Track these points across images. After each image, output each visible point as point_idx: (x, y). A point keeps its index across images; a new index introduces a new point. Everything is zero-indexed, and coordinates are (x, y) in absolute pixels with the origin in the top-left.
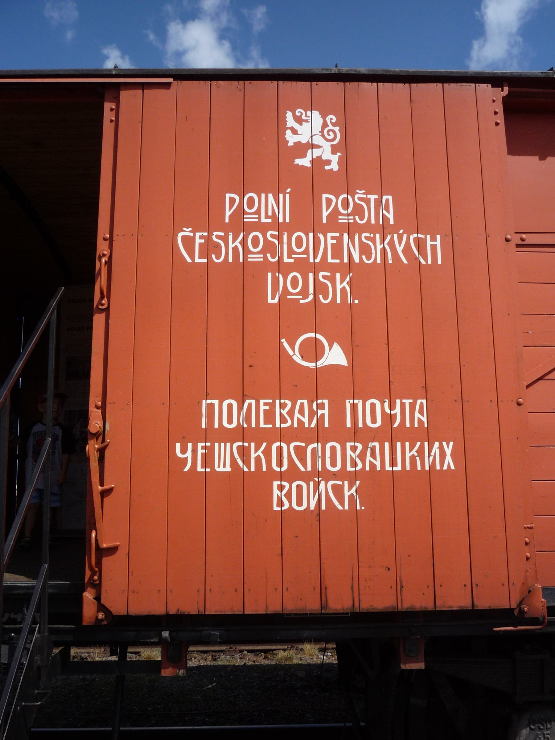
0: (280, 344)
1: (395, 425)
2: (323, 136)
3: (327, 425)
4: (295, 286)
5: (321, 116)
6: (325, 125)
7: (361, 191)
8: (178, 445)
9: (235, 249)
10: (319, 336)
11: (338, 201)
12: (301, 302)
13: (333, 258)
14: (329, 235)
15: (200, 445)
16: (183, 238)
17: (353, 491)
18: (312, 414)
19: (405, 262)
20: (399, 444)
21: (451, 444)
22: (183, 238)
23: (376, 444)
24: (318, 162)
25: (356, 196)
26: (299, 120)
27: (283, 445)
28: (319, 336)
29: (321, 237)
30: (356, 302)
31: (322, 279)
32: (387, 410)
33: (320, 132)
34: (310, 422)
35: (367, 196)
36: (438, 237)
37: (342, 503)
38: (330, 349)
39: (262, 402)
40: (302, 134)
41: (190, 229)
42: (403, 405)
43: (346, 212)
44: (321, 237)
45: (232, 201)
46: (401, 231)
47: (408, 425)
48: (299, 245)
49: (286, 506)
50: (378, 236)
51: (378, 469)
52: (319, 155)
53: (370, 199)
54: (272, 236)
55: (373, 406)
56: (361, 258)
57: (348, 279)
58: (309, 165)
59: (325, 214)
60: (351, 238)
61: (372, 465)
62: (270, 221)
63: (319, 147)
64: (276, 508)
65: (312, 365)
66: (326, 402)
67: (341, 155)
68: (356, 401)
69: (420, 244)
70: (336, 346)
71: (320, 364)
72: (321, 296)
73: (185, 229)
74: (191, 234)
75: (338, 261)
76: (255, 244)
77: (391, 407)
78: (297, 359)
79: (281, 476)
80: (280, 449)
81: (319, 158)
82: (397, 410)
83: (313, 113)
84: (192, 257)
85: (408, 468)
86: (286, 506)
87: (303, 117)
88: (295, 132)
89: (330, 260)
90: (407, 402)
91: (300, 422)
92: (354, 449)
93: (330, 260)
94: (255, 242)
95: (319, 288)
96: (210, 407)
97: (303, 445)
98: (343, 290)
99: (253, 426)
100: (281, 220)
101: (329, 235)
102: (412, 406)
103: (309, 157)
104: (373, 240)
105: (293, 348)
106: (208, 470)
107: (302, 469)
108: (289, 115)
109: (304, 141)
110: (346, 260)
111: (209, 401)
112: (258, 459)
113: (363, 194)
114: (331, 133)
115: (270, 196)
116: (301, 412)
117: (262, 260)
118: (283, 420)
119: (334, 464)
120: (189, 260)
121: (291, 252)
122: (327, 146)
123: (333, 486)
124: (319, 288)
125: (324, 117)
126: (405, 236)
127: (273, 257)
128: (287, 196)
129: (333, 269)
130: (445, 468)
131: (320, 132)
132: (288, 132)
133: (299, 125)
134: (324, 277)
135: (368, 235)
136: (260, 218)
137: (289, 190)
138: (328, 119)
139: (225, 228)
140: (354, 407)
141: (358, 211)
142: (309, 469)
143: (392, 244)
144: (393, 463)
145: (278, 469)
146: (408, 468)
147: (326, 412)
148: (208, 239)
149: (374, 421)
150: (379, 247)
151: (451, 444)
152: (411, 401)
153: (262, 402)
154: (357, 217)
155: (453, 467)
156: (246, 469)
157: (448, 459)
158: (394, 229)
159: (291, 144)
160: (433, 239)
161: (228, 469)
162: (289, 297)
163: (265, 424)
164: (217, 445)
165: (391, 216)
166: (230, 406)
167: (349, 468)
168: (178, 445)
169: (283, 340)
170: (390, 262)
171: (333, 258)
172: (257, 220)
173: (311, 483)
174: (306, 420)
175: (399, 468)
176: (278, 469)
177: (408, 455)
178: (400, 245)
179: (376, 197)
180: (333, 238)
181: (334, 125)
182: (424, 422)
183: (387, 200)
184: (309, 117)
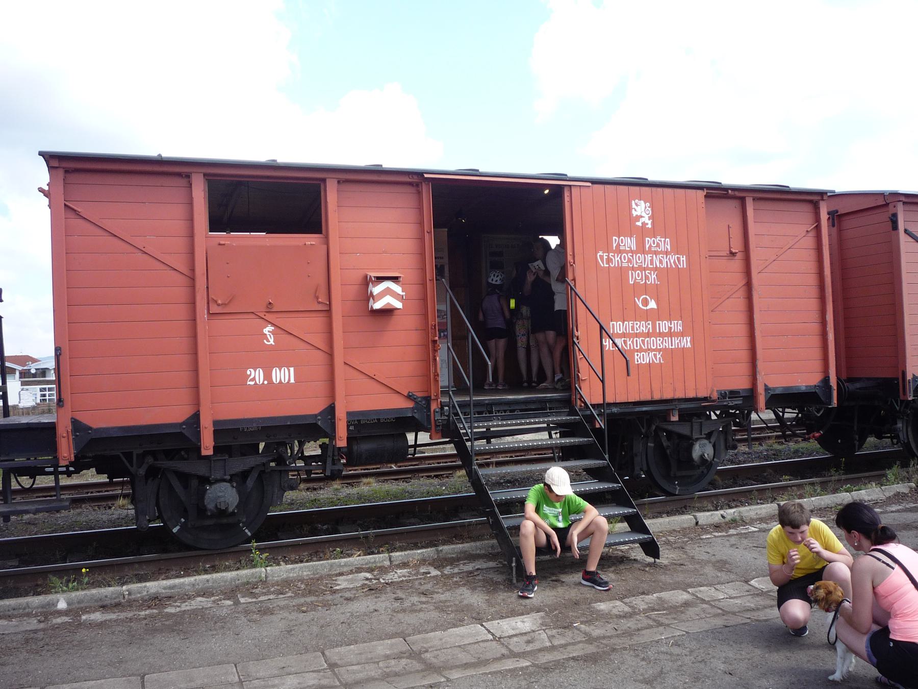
0: (635, 300)
4: (638, 276)
12: (641, 283)
18: (646, 327)
65: (645, 308)
78: (641, 305)
169: (636, 298)
174: (644, 329)
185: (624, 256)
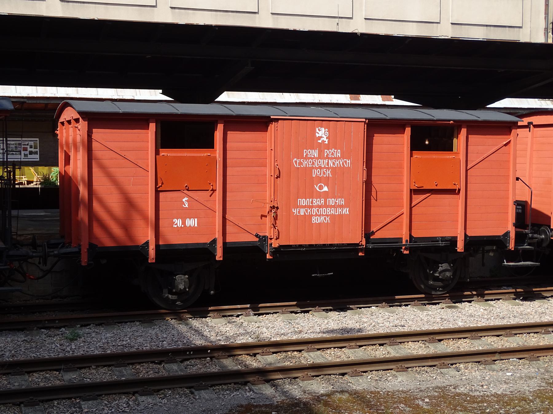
4: (318, 173)
6: (325, 132)
8: (293, 209)
10: (322, 184)
13: (327, 166)
14: (326, 160)
16: (295, 161)
18: (320, 202)
22: (295, 161)
23: (333, 209)
24: (323, 141)
26: (319, 130)
28: (322, 184)
29: (324, 160)
31: (324, 171)
36: (349, 160)
37: (326, 221)
39: (310, 199)
42: (339, 200)
43: (330, 154)
44: (324, 160)
49: (315, 222)
51: (333, 214)
55: (333, 200)
58: (321, 142)
61: (332, 213)
62: (313, 157)
63: (323, 137)
66: (323, 199)
69: (346, 162)
70: (326, 186)
71: (322, 191)
75: (328, 166)
76: (310, 163)
77: (337, 200)
78: (318, 189)
81: (323, 140)
82: (338, 201)
84: (297, 165)
88: (318, 133)
89: (326, 166)
90: (340, 199)
91: (318, 204)
93: (326, 166)
95: (324, 173)
98: (329, 173)
99: (308, 205)
101: (326, 160)
102: (341, 200)
103: (321, 140)
105: (317, 187)
108: (317, 129)
109: (320, 136)
110: (330, 166)
112: (309, 212)
119: (324, 213)
120: (296, 166)
122: (325, 137)
124: (324, 173)
125: (325, 129)
129: (327, 168)
130: (347, 214)
132: (317, 133)
134: (325, 170)
137: (318, 149)
139: (304, 158)
140: (329, 200)
141: (333, 154)
142: (320, 214)
143: (339, 162)
147: (323, 201)
149: (333, 203)
153: (310, 199)
155: (348, 214)
157: (348, 212)
158: (340, 158)
159: (317, 136)
160: (348, 161)
161: (303, 214)
166: (304, 200)
168: (293, 209)
171: (327, 166)
174: (319, 203)
175: (337, 214)
177: (339, 211)
180: (327, 161)
181: (327, 131)
185: (310, 161)
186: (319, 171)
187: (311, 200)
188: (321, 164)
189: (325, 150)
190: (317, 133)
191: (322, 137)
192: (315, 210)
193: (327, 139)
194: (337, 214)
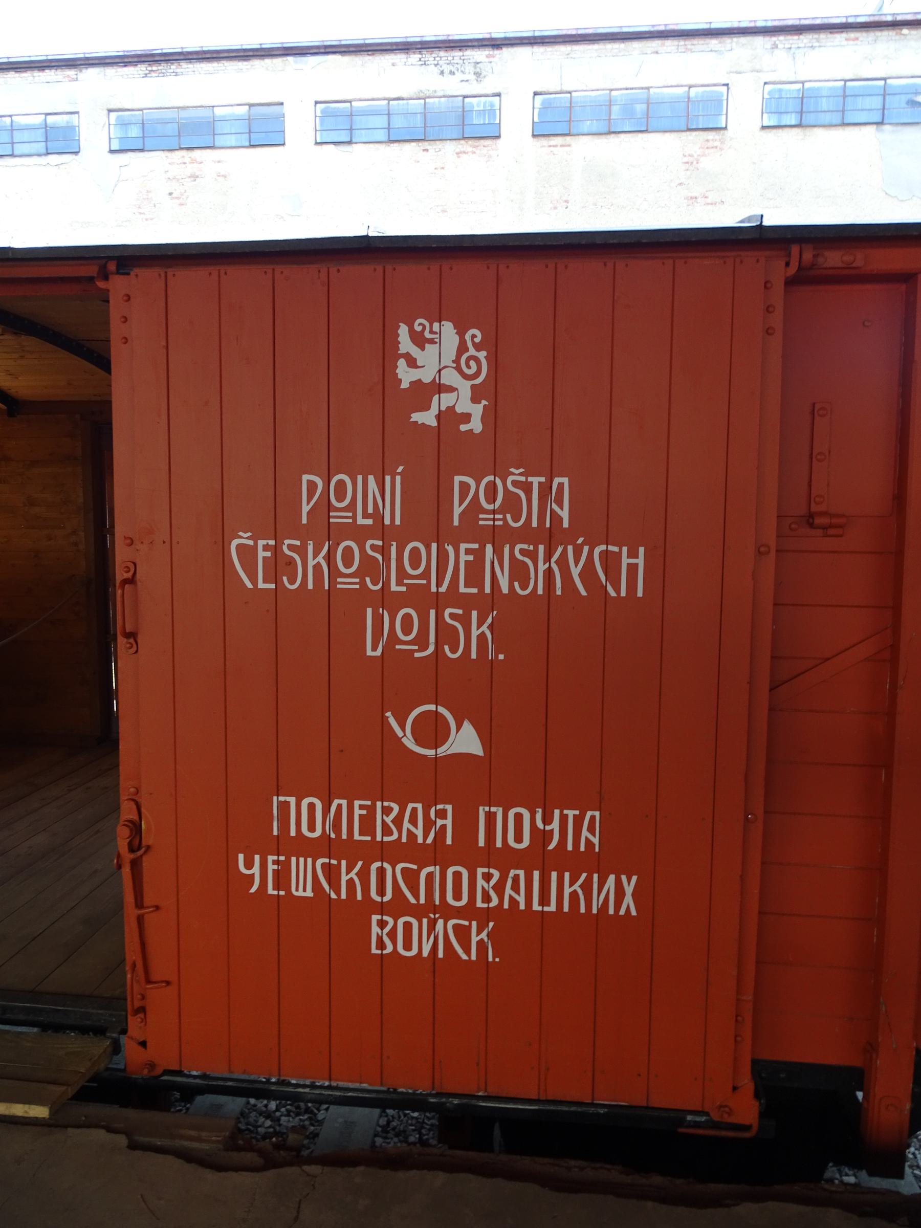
0: (384, 720)
1: (551, 847)
2: (458, 369)
3: (449, 841)
4: (407, 630)
5: (456, 331)
7: (517, 469)
8: (241, 857)
9: (317, 567)
10: (441, 710)
11: (478, 488)
12: (417, 655)
14: (463, 547)
15: (271, 858)
17: (484, 935)
18: (428, 824)
19: (584, 593)
20: (554, 875)
21: (634, 878)
22: (239, 547)
23: (521, 873)
24: (449, 417)
25: (510, 479)
26: (419, 340)
27: (386, 865)
28: (441, 710)
29: (450, 549)
30: (501, 657)
32: (540, 825)
33: (453, 362)
34: (425, 837)
35: (527, 479)
36: (642, 550)
37: (468, 951)
38: (458, 729)
39: (357, 803)
40: (424, 366)
41: (249, 534)
42: (564, 819)
43: (490, 507)
44: (450, 549)
45: (312, 486)
46: (580, 541)
47: (570, 847)
48: (415, 564)
49: (389, 949)
50: (541, 548)
51: (522, 907)
52: (451, 404)
53: (532, 483)
54: (373, 547)
55: (519, 818)
56: (511, 587)
57: (489, 620)
59: (457, 510)
60: (498, 553)
61: (514, 902)
62: (369, 522)
63: (451, 389)
64: (374, 951)
65: (430, 753)
67: (487, 403)
68: (493, 809)
69: (610, 562)
70: (467, 727)
72: (446, 648)
73: (240, 534)
74: (251, 543)
76: (348, 563)
77: (547, 820)
78: (409, 743)
79: (382, 908)
80: (381, 872)
81: (451, 409)
82: (555, 826)
83: (443, 325)
84: (253, 579)
85: (566, 909)
86: (389, 949)
87: (427, 335)
88: (412, 363)
89: (462, 589)
90: (571, 813)
91: (411, 836)
92: (487, 877)
93: (462, 589)
94: (348, 558)
95: (446, 635)
96: (284, 806)
97: (415, 867)
98: (482, 638)
99: (344, 837)
100: (387, 521)
101: (463, 547)
102: (578, 821)
104: (533, 556)
106: (282, 893)
107: (413, 901)
108: (403, 330)
109: (427, 380)
110: (488, 590)
111: (282, 799)
112: (350, 882)
113: (520, 474)
114: (472, 363)
115: (371, 478)
116: (413, 821)
117: (357, 586)
118: (386, 831)
121: (402, 574)
122: (465, 388)
123: (455, 927)
124: (446, 635)
125: (461, 333)
126: (586, 549)
127: (375, 583)
128: (398, 478)
130: (622, 912)
131: (453, 362)
132: (402, 363)
133: (419, 350)
134: (453, 616)
135: (525, 546)
136: (354, 517)
137: (400, 469)
138: (468, 337)
140: (491, 817)
142: (422, 901)
143: (563, 563)
144: (544, 899)
145: (378, 899)
146: (566, 909)
147: (449, 822)
148: (276, 550)
149: (519, 838)
150: (542, 567)
151: (634, 878)
152: (577, 812)
153: (357, 803)
154: (508, 516)
156: (333, 896)
157: (628, 900)
158: (568, 537)
159: (405, 385)
160: (633, 554)
161: (309, 893)
162: (397, 647)
163: (360, 835)
164: (294, 859)
165: (565, 514)
166: (311, 807)
167: (480, 904)
168: (241, 857)
170: (559, 592)
172: (351, 521)
173: (425, 921)
174: (419, 833)
175: (552, 908)
176: (378, 899)
177: (567, 891)
178: (576, 565)
179: (543, 479)
180: (468, 551)
181: (478, 347)
182: (594, 845)
183: (561, 486)
184: (436, 333)
185: (348, 551)
186: (407, 617)
187: (361, 807)
188: (426, 574)
189: (458, 479)
190: (402, 363)
191: (439, 388)
192: (394, 872)
193: (475, 399)
194: (552, 908)
